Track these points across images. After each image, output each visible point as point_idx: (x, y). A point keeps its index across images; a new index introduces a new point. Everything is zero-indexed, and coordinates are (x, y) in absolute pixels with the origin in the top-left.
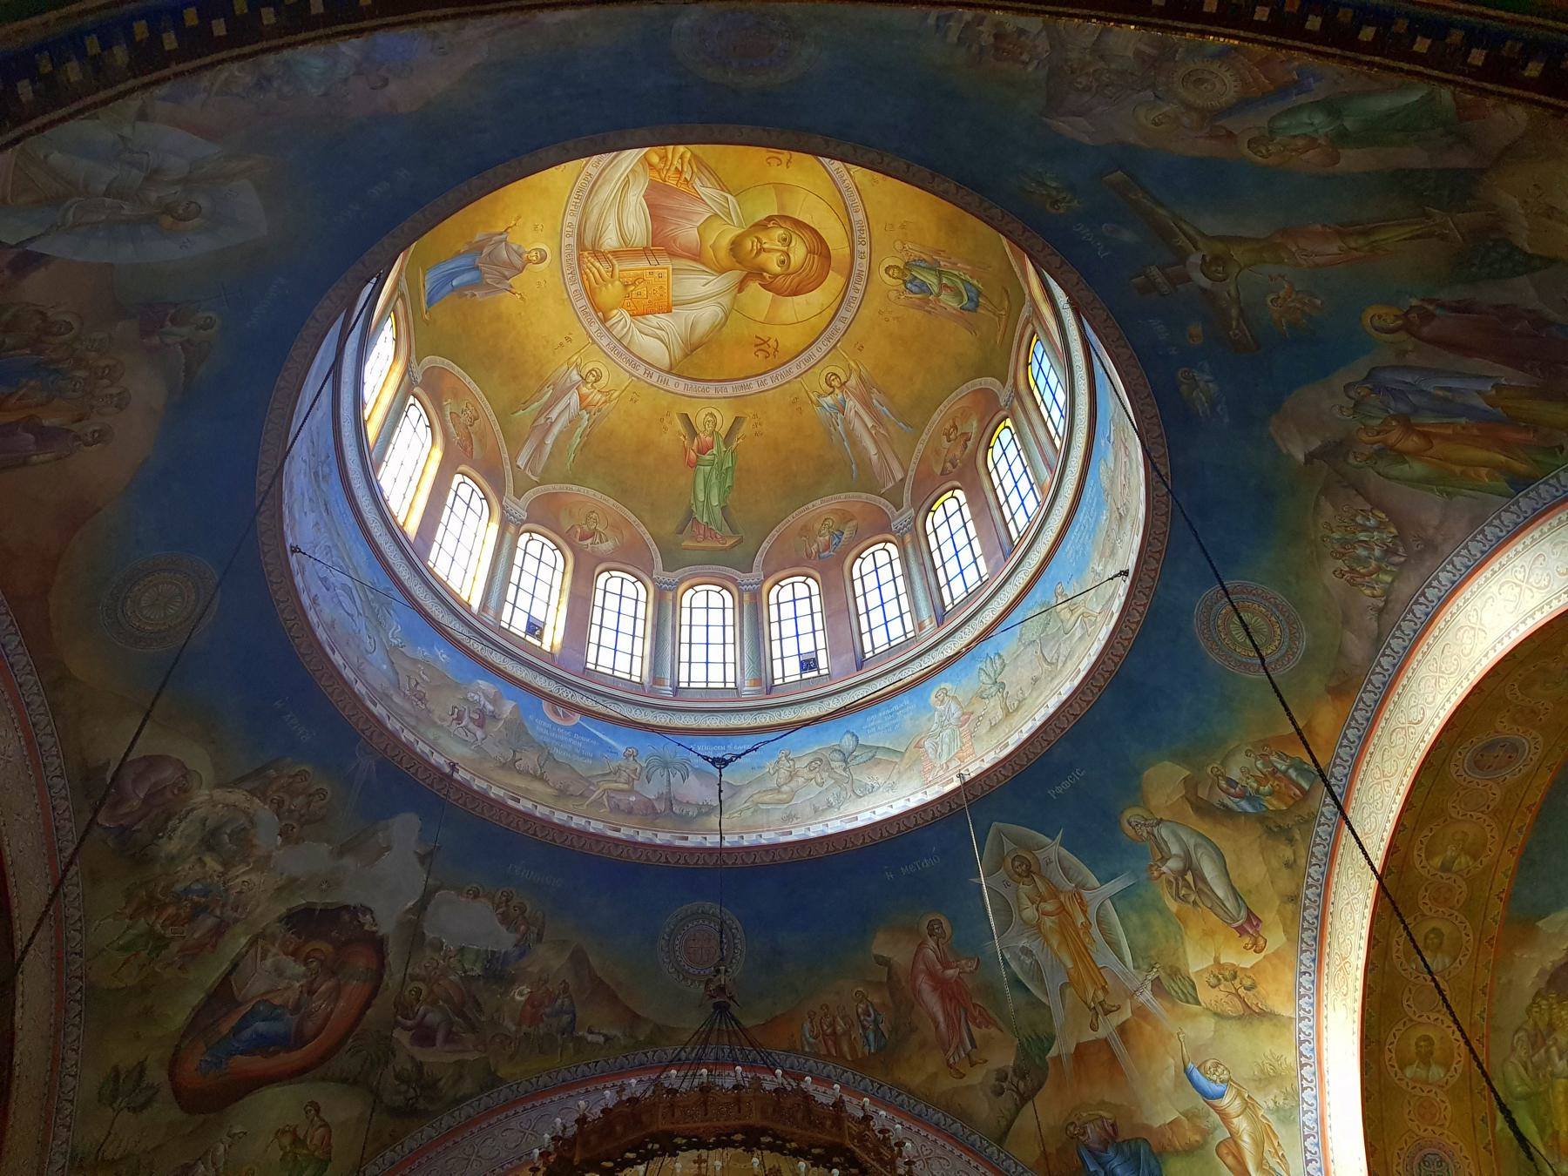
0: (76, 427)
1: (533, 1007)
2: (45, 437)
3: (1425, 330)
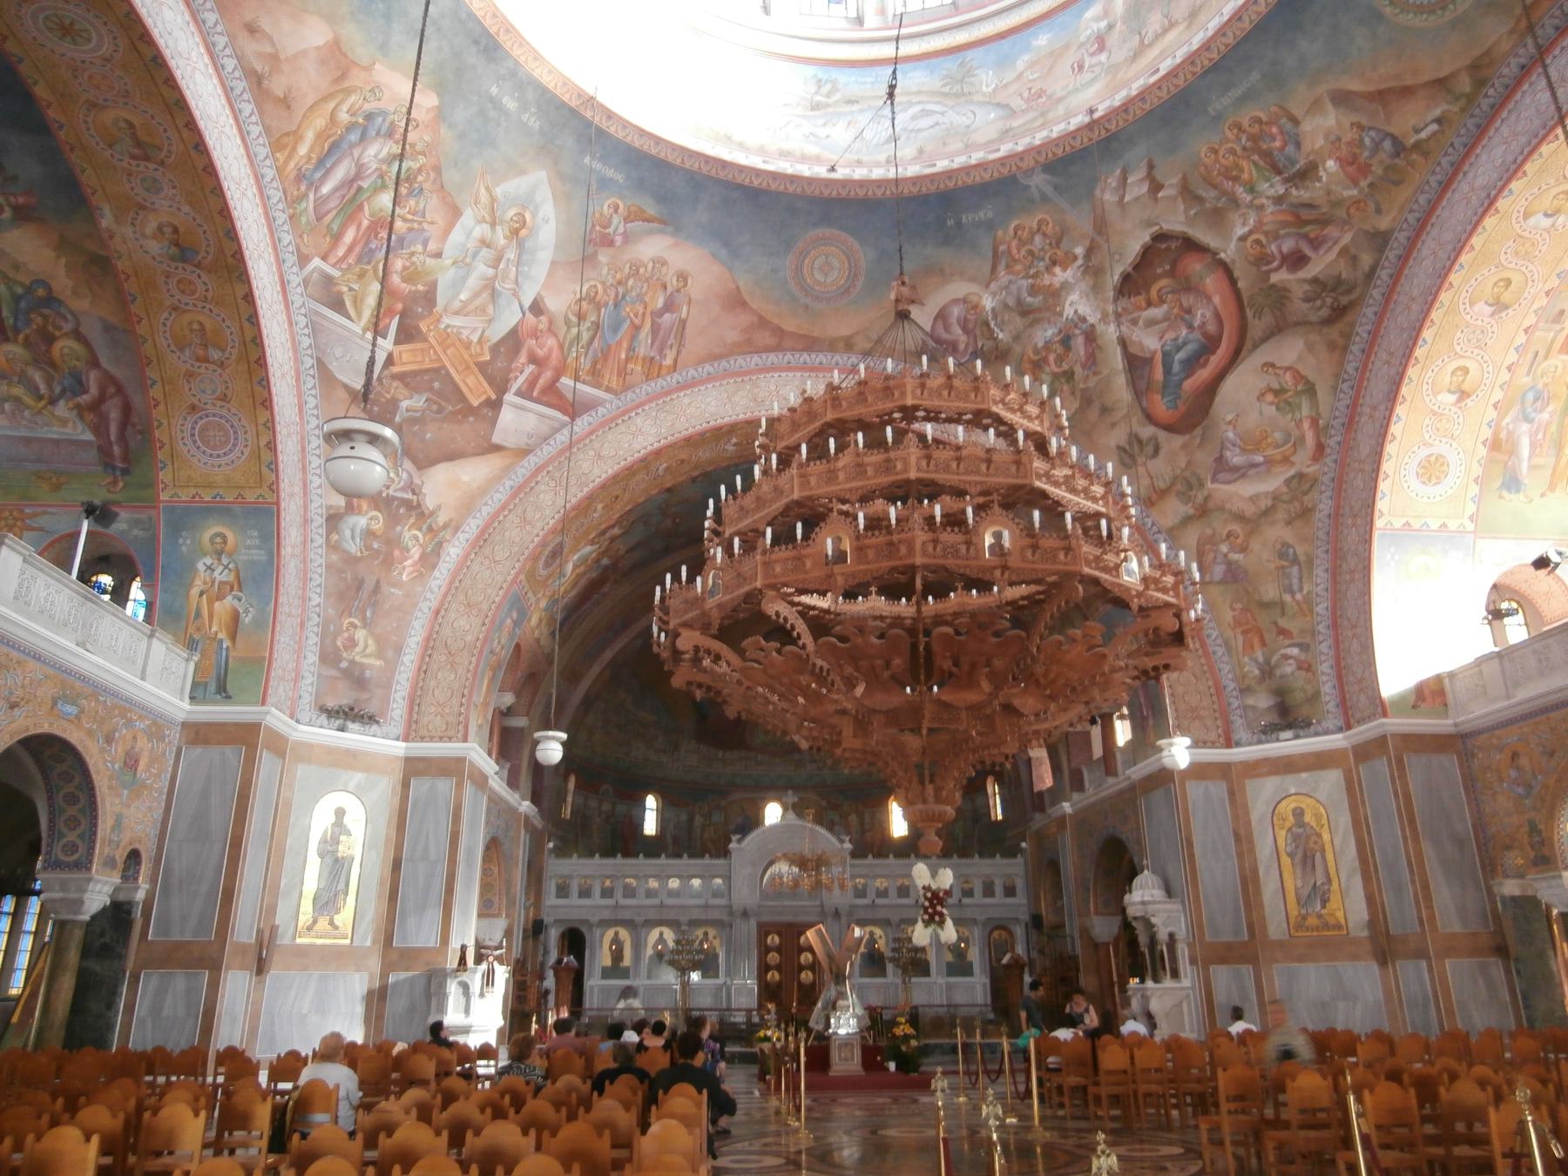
0: (670, 290)
1: (1352, 164)
2: (669, 306)
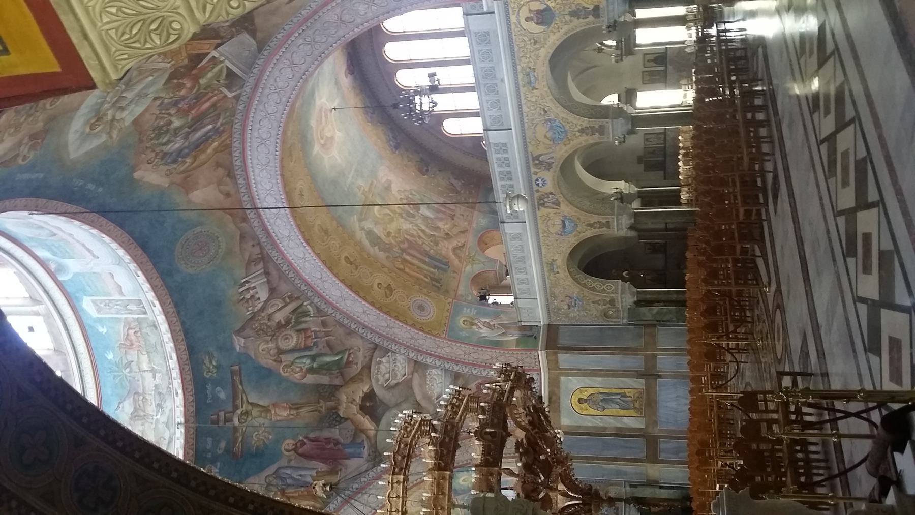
3: (301, 451)
